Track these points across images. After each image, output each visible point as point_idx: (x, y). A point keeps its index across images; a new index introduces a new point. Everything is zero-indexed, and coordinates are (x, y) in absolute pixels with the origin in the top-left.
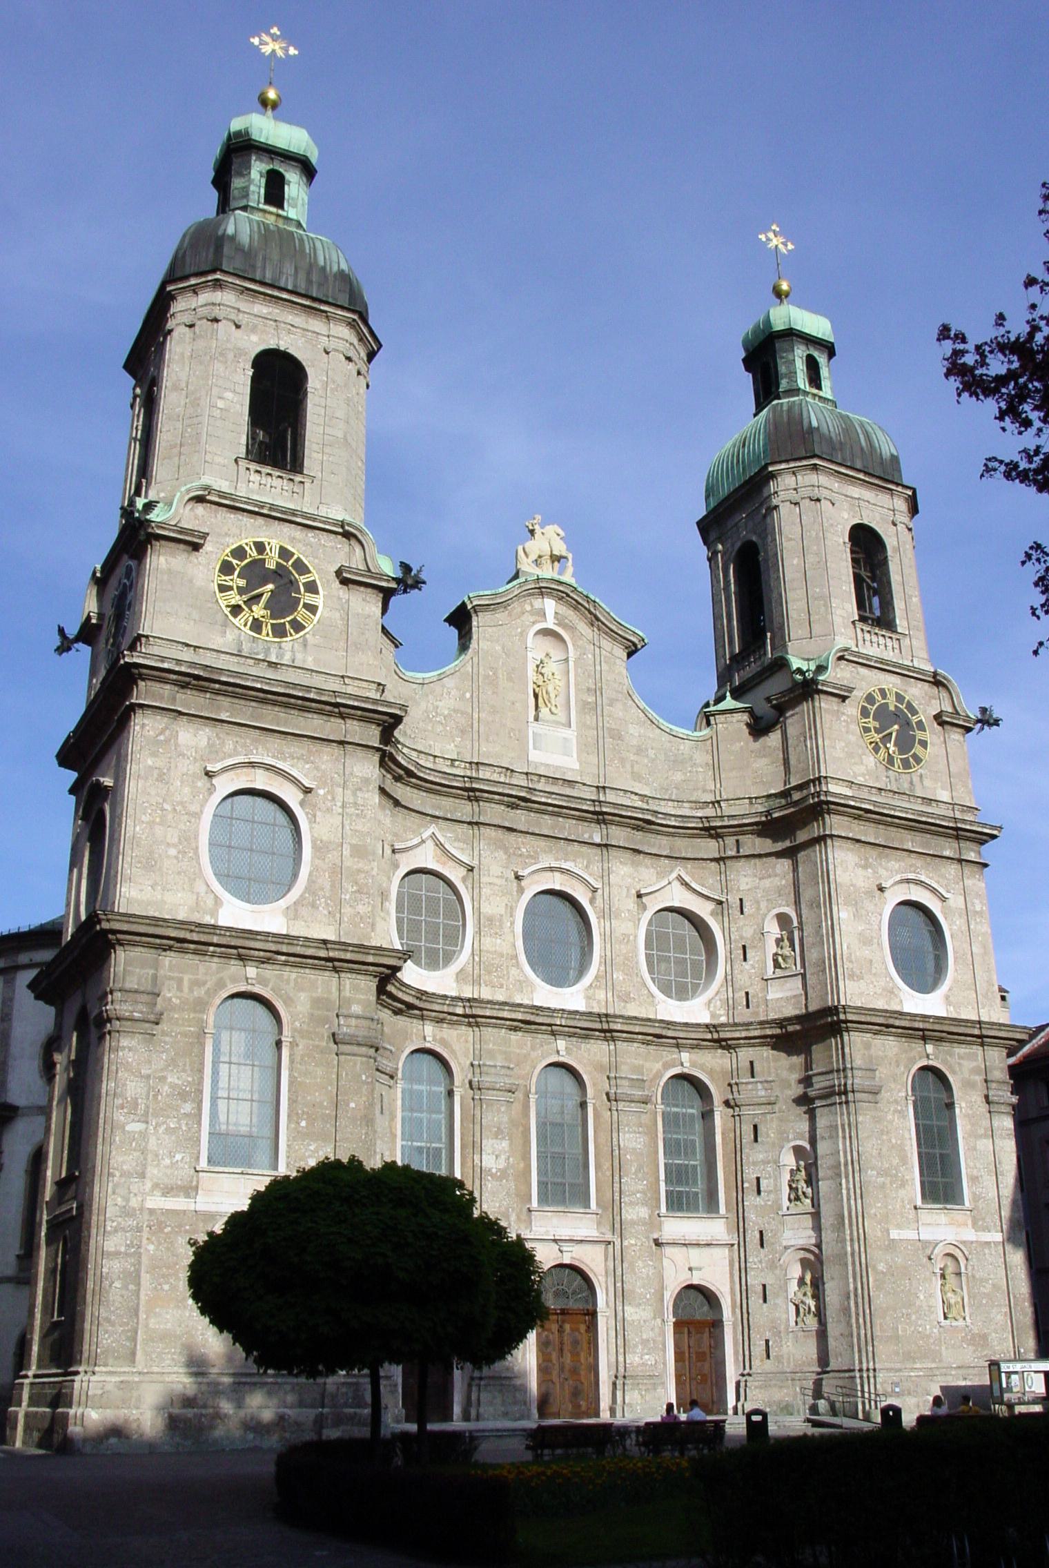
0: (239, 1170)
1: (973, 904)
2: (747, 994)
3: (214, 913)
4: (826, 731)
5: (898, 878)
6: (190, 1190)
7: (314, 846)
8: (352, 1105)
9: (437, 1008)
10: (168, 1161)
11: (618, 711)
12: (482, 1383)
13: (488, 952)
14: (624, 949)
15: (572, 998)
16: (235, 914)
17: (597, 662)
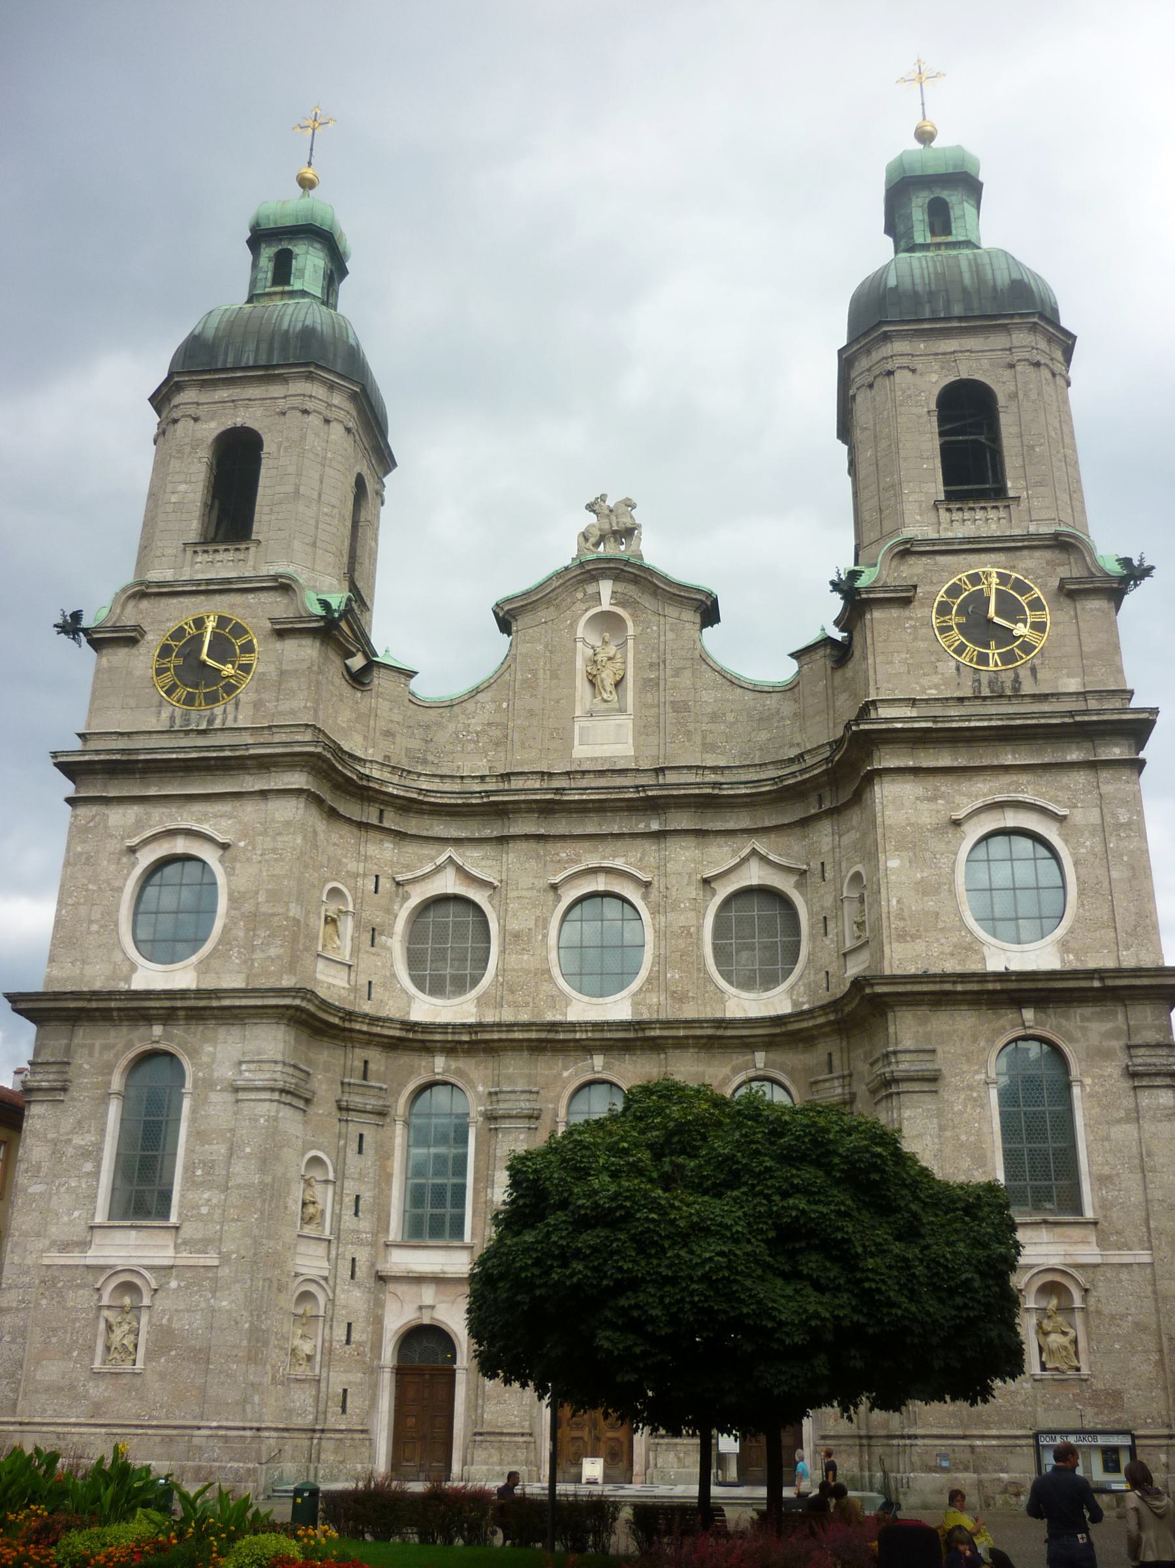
0: (128, 1223)
1: (1114, 815)
2: (827, 973)
3: (128, 979)
4: (879, 646)
5: (979, 803)
6: (84, 1245)
7: (232, 899)
8: (248, 1150)
9: (438, 1037)
10: (66, 1219)
11: (686, 679)
12: (478, 1438)
13: (514, 970)
14: (681, 943)
15: (617, 1008)
16: (150, 977)
17: (662, 633)
